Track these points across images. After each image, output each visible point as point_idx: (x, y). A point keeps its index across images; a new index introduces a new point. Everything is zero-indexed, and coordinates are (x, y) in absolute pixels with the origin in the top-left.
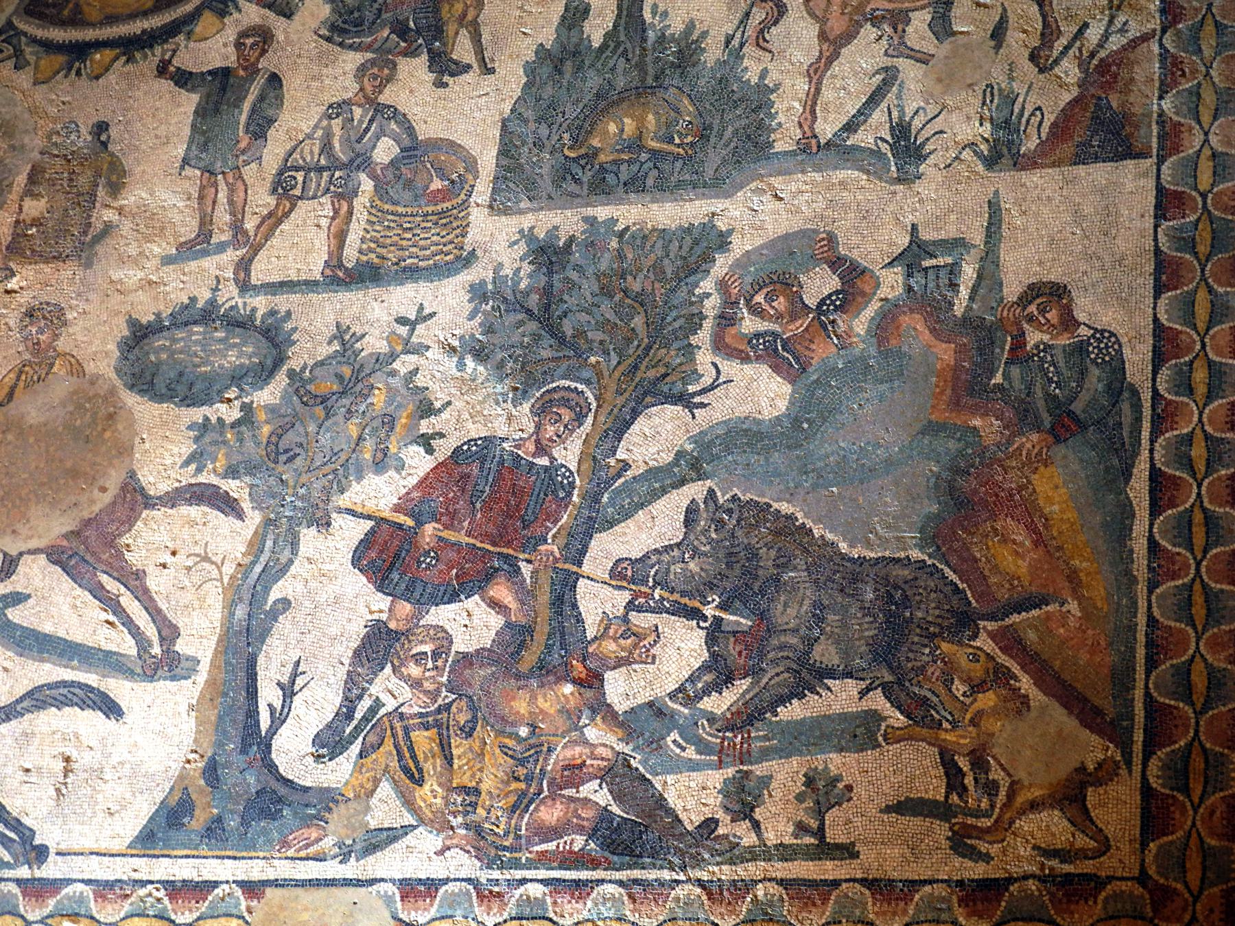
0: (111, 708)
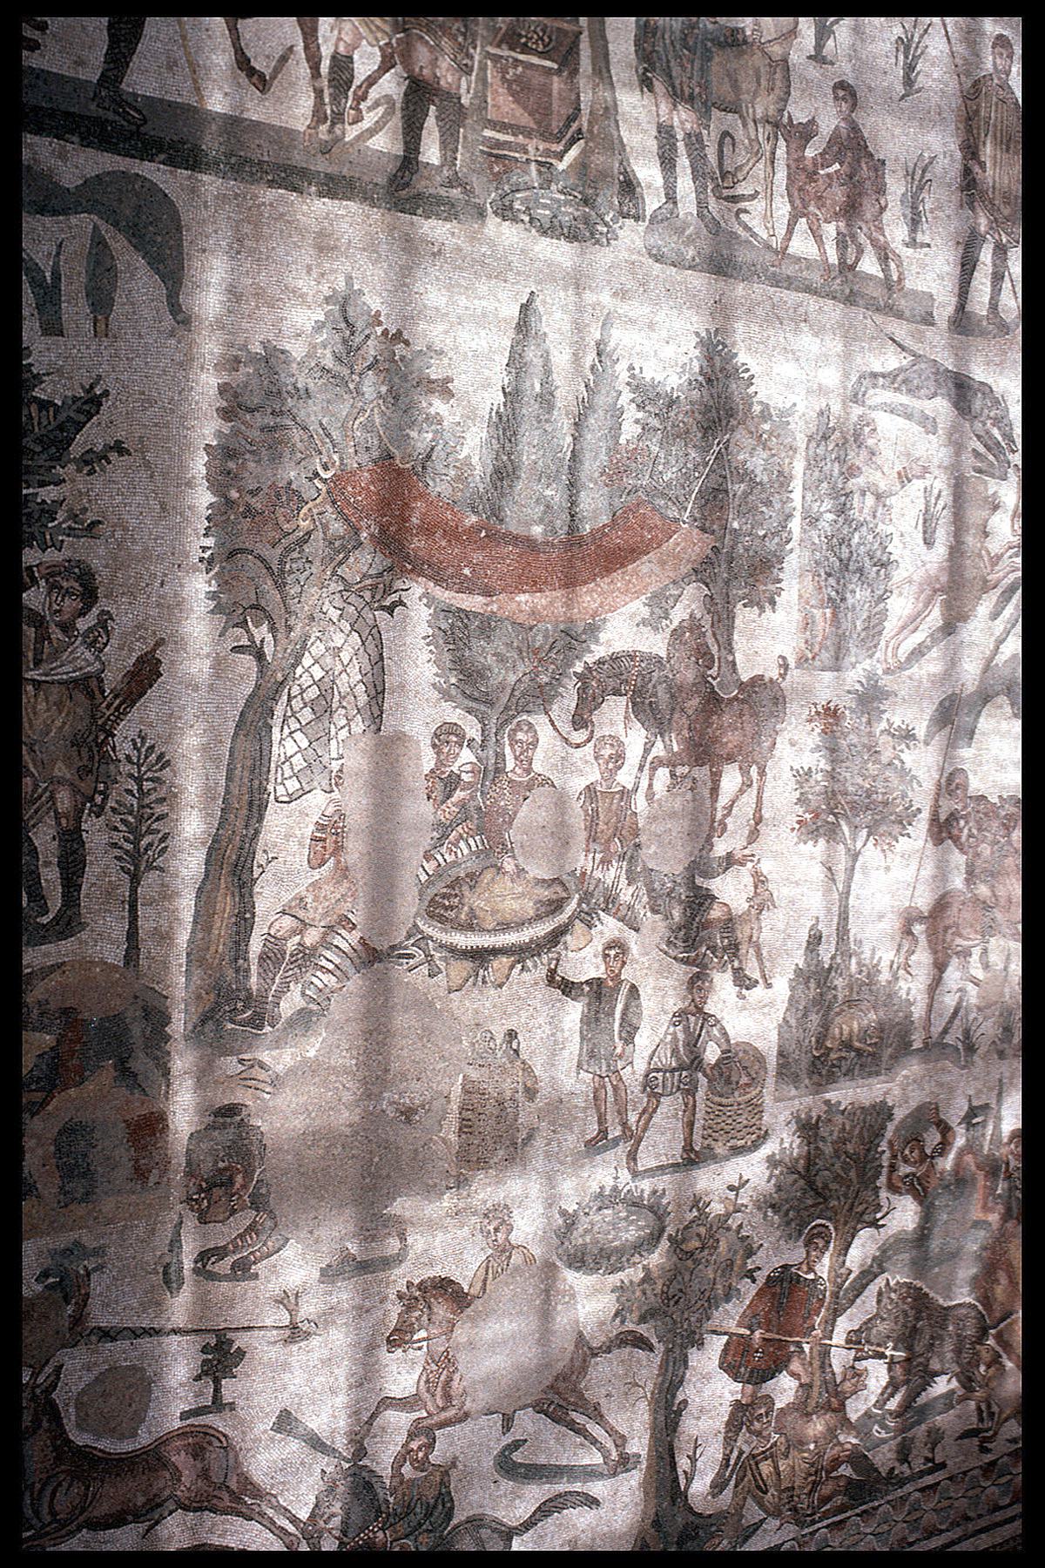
0: (593, 1502)
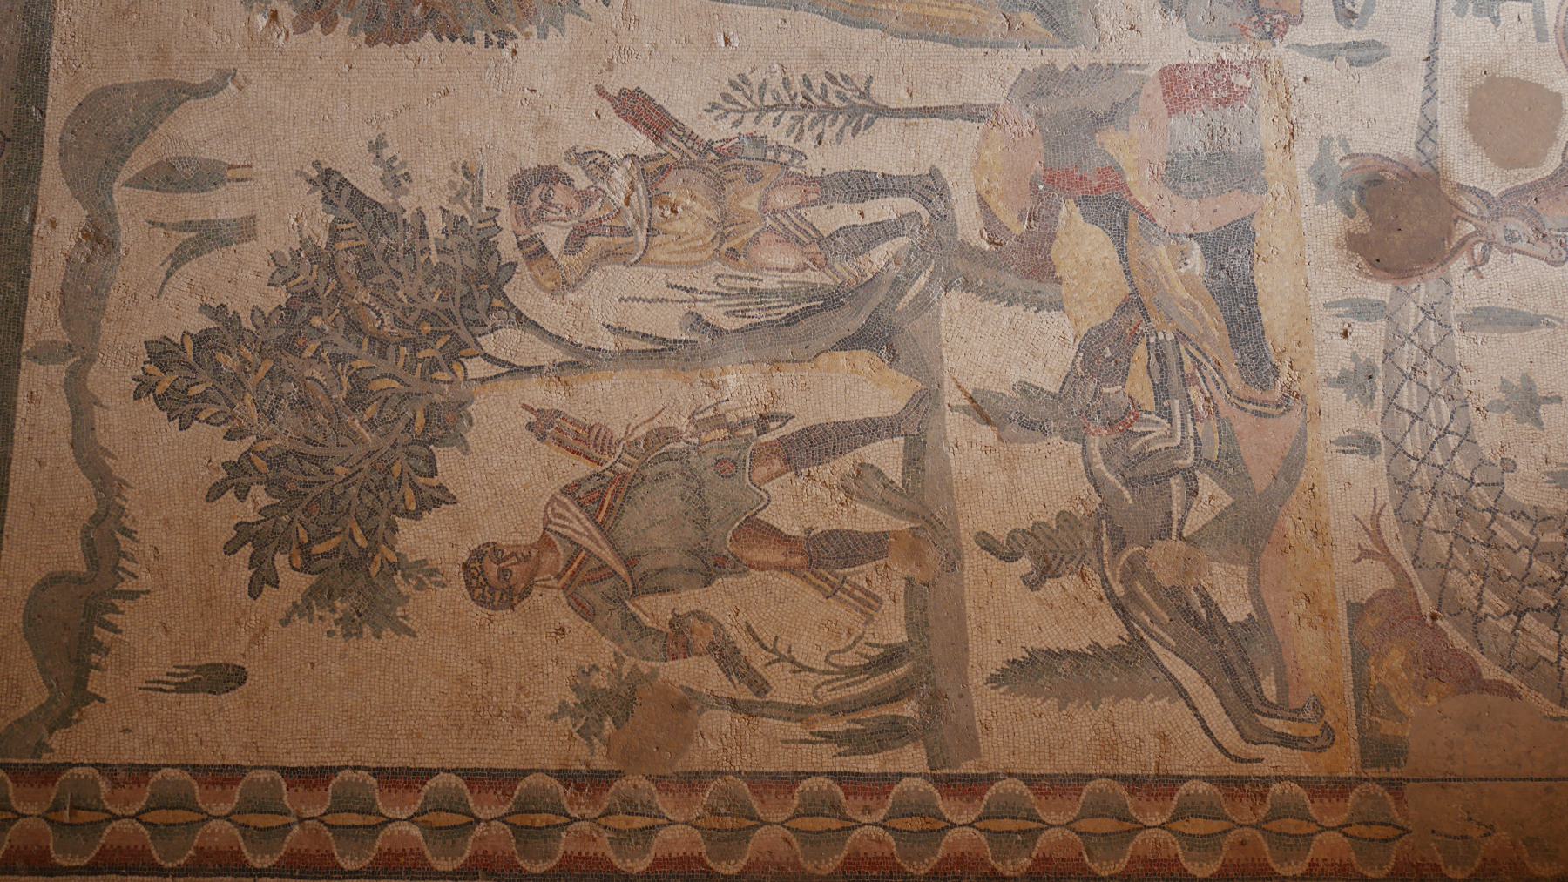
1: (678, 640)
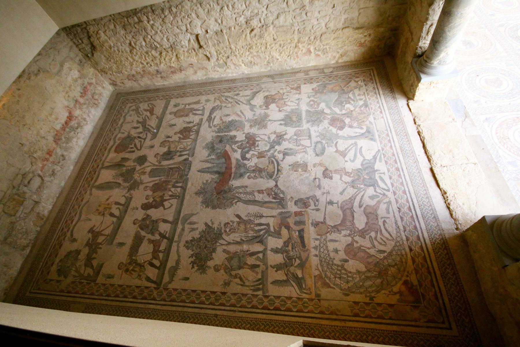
0: (361, 148)
1: (236, 277)
